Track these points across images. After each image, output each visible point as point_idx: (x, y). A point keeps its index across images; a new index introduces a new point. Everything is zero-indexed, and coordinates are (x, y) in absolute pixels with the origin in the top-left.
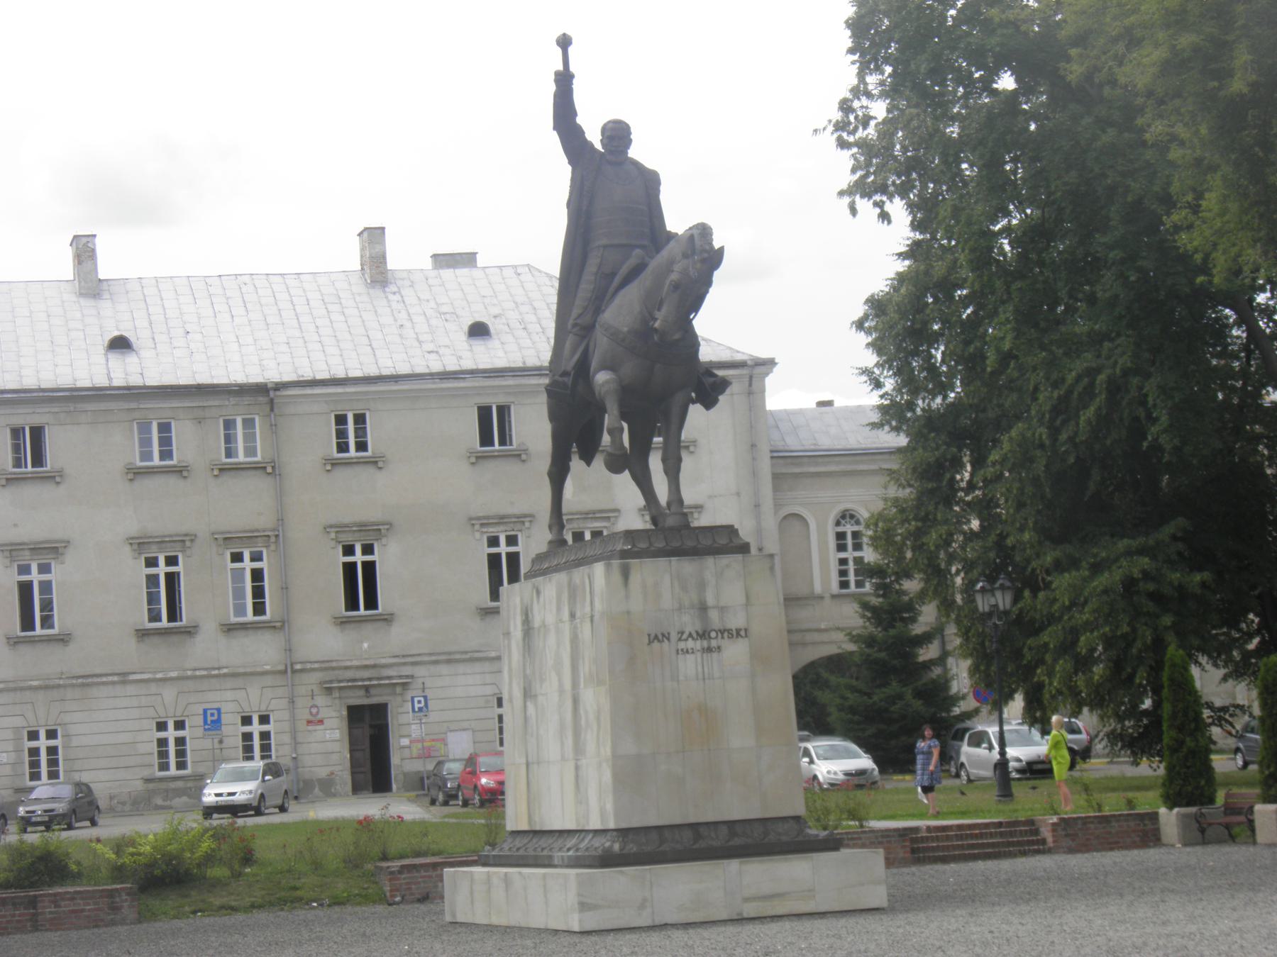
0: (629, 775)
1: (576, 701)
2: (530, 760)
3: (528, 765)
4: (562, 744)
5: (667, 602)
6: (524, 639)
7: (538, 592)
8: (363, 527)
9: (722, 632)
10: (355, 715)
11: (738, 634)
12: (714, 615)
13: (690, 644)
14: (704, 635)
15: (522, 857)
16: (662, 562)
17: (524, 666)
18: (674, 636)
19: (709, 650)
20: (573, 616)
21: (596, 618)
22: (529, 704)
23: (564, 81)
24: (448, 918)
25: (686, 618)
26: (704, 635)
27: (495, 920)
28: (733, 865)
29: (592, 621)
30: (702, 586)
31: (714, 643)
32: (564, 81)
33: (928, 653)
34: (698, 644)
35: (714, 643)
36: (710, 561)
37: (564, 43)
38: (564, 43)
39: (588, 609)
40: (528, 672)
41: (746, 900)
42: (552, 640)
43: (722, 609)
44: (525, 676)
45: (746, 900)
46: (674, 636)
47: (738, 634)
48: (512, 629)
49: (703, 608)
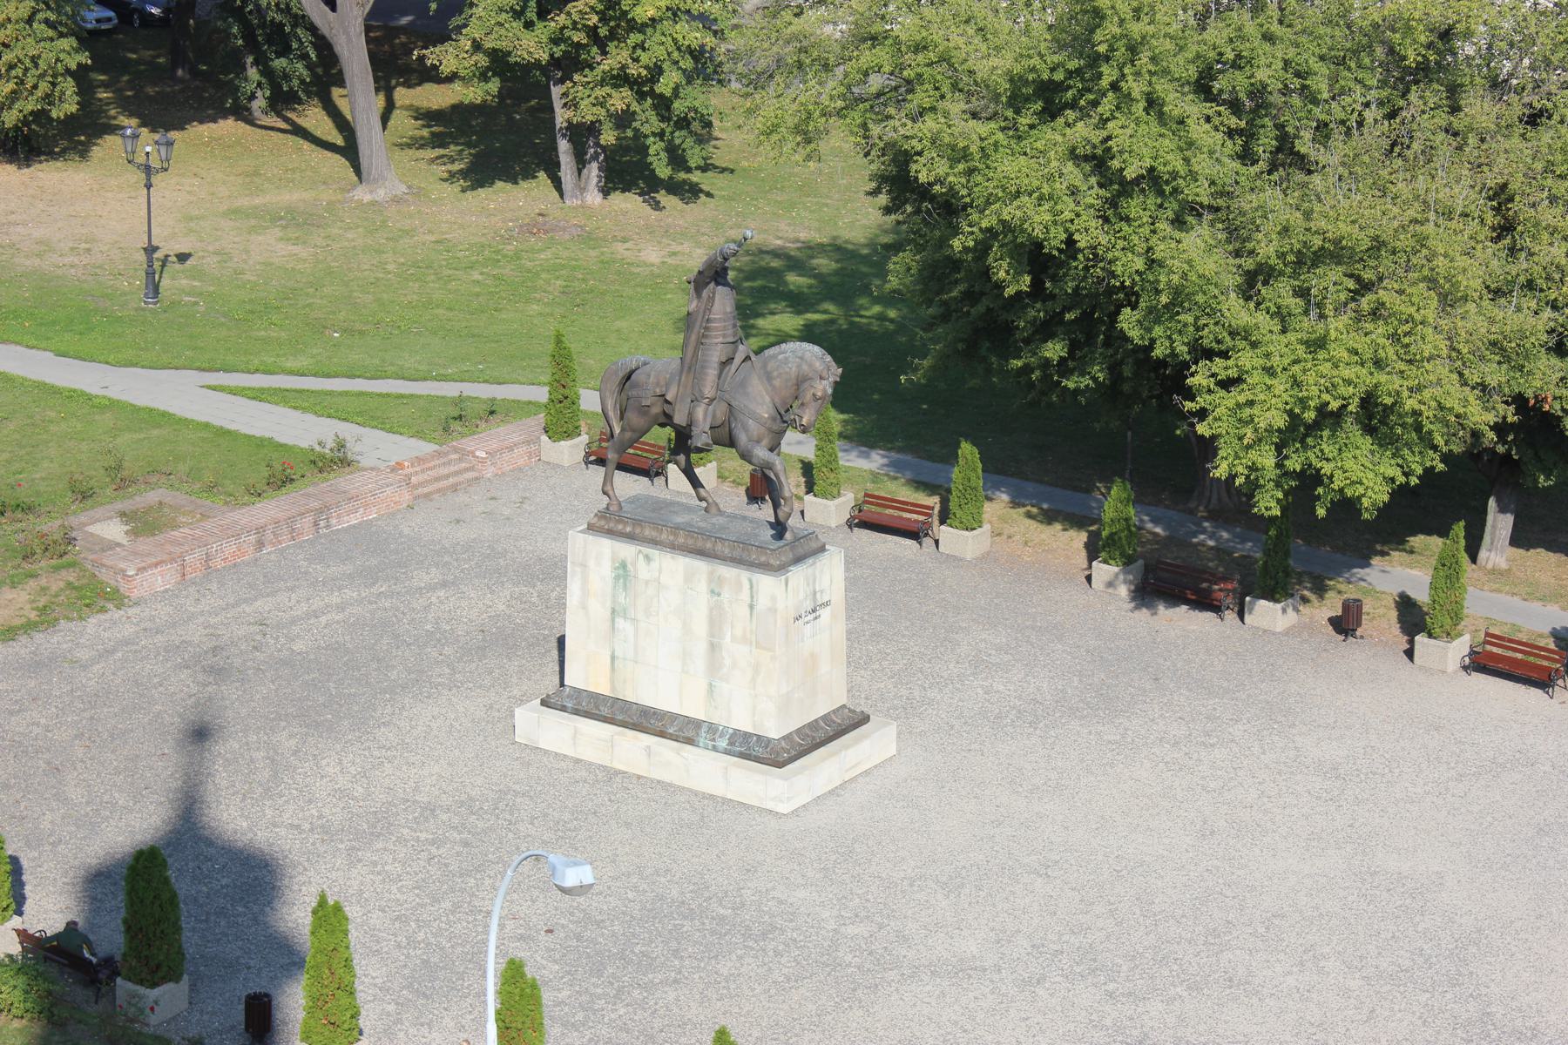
1: (713, 647)
3: (613, 658)
6: (617, 578)
21: (758, 608)
26: (814, 611)
29: (751, 607)
34: (810, 617)
40: (621, 599)
44: (614, 602)
47: (827, 604)
48: (591, 563)
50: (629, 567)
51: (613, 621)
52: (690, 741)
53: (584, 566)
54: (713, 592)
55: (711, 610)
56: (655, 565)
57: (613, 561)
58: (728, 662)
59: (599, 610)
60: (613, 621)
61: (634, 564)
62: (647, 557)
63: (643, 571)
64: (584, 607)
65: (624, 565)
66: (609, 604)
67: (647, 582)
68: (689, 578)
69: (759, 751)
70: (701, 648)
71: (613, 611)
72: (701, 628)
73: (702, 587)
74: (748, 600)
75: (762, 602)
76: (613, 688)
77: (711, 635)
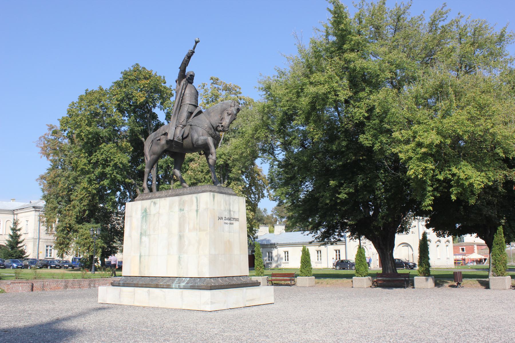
0: (213, 261)
1: (181, 237)
2: (143, 254)
3: (140, 257)
5: (222, 208)
6: (143, 218)
9: (234, 219)
11: (237, 220)
12: (232, 213)
14: (230, 219)
15: (146, 284)
16: (222, 195)
17: (142, 226)
18: (224, 219)
19: (231, 224)
20: (181, 210)
21: (200, 211)
24: (99, 302)
25: (226, 213)
27: (136, 304)
28: (244, 289)
29: (197, 211)
30: (230, 204)
31: (232, 222)
33: (19, 245)
35: (232, 222)
36: (232, 197)
39: (194, 207)
40: (144, 227)
41: (247, 301)
43: (234, 212)
44: (141, 229)
45: (247, 301)
46: (224, 219)
47: (237, 220)
49: (230, 211)
50: (148, 210)
51: (141, 238)
52: (168, 287)
53: (131, 216)
54: (181, 210)
55: (180, 218)
56: (157, 205)
57: (142, 210)
60: (141, 238)
61: (150, 208)
64: (130, 236)
65: (146, 211)
66: (139, 232)
67: (154, 215)
68: (171, 207)
69: (199, 284)
70: (175, 239)
71: (141, 234)
72: (175, 230)
73: (176, 209)
75: (202, 206)
76: (140, 272)
77: (180, 231)
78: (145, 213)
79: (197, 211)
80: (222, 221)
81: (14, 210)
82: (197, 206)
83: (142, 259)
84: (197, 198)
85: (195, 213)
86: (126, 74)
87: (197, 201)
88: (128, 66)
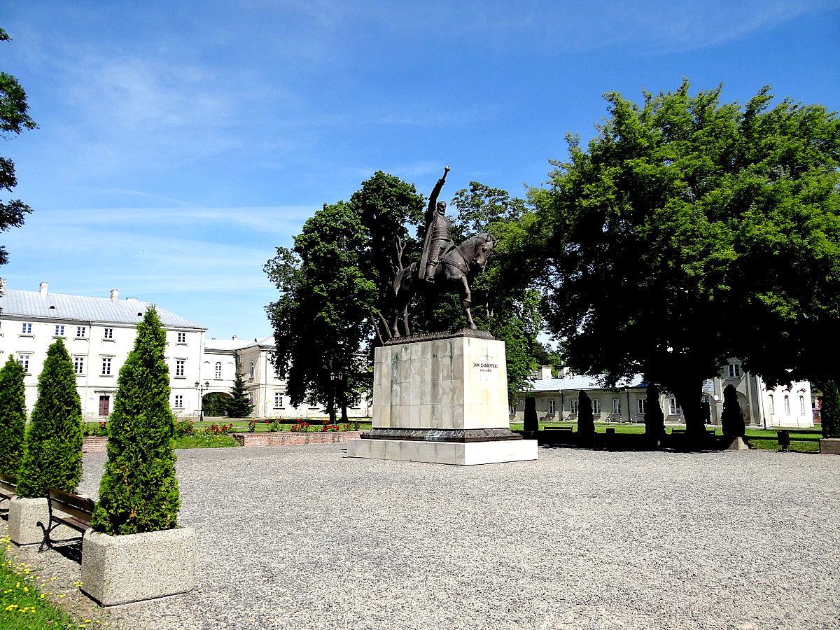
1: (435, 385)
2: (394, 404)
4: (421, 399)
7: (406, 349)
8: (108, 356)
10: (101, 398)
11: (495, 366)
13: (484, 368)
14: (487, 366)
15: (398, 437)
18: (480, 365)
22: (394, 386)
23: (441, 183)
29: (451, 357)
31: (490, 369)
32: (441, 183)
34: (487, 368)
37: (447, 170)
38: (447, 170)
39: (448, 353)
42: (417, 365)
44: (392, 376)
47: (495, 366)
51: (392, 386)
54: (434, 356)
56: (409, 351)
58: (441, 392)
59: (386, 382)
60: (392, 386)
62: (406, 349)
63: (404, 356)
67: (406, 361)
68: (424, 352)
70: (429, 387)
72: (428, 377)
74: (449, 354)
76: (391, 424)
77: (433, 380)
78: (397, 358)
79: (451, 357)
80: (479, 368)
81: (236, 350)
82: (451, 351)
83: (393, 409)
84: (451, 343)
85: (449, 359)
86: (367, 185)
87: (451, 346)
88: (368, 175)
